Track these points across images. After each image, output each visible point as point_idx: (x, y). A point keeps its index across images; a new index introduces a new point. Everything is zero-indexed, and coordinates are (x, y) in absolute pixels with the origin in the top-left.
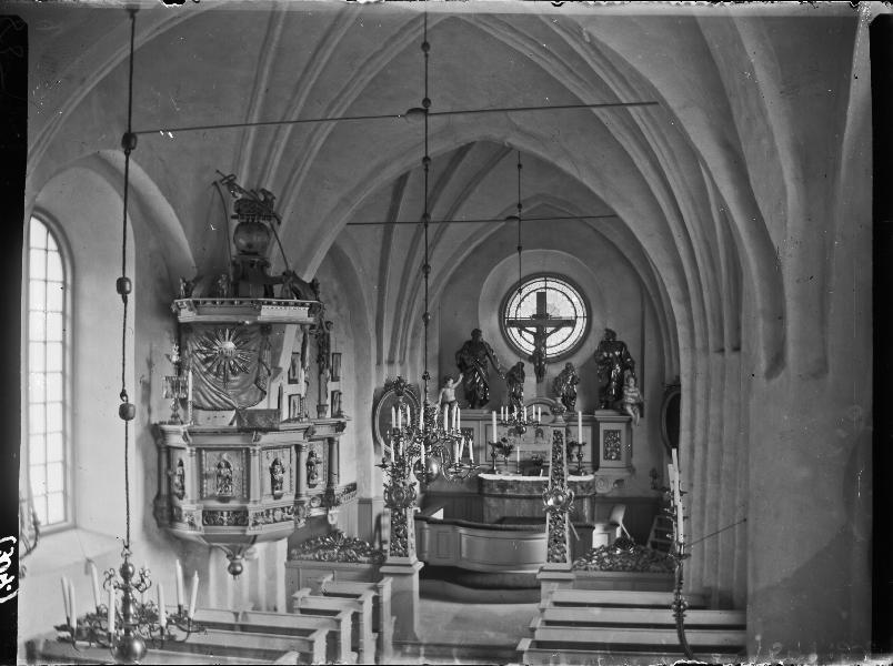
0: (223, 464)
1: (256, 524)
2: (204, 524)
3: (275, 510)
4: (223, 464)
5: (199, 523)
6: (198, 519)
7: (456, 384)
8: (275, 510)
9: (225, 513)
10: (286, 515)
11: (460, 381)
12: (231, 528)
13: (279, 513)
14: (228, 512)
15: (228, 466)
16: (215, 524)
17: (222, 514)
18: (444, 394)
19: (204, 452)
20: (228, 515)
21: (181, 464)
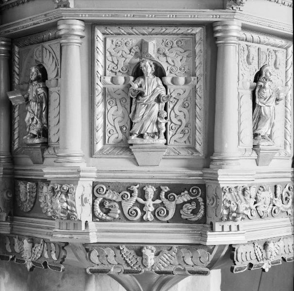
0: (149, 69)
1: (232, 216)
2: (94, 216)
3: (261, 188)
4: (149, 69)
5: (84, 213)
6: (84, 201)
9: (151, 191)
10: (278, 203)
12: (157, 226)
14: (159, 190)
15: (159, 73)
16: (124, 218)
17: (143, 194)
19: (99, 33)
20: (157, 196)
21: (43, 77)
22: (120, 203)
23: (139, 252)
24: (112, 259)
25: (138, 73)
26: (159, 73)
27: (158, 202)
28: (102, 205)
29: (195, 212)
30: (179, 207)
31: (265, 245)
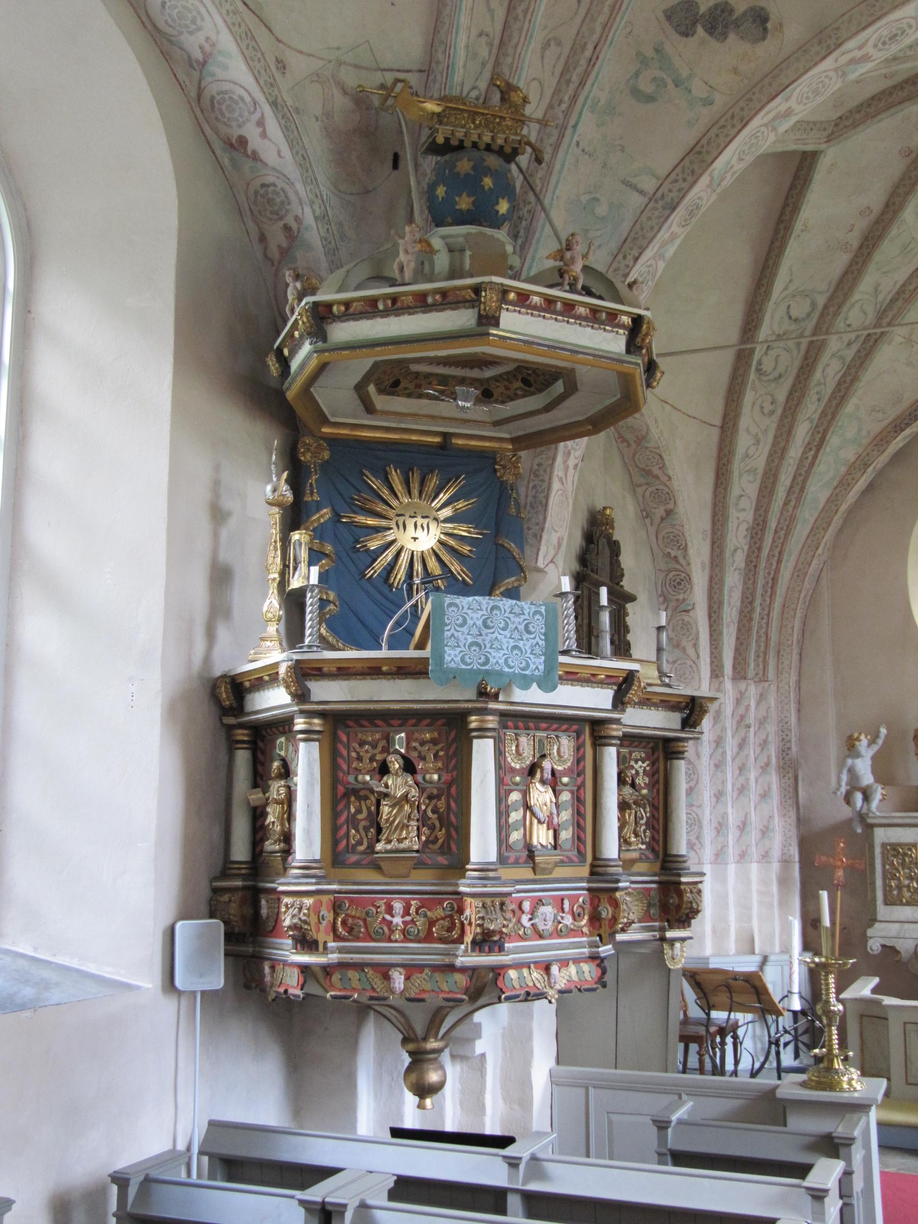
0: (396, 764)
4: (396, 764)
7: (875, 748)
8: (539, 902)
9: (398, 906)
10: (568, 920)
11: (880, 742)
13: (548, 911)
17: (390, 910)
18: (851, 771)
20: (406, 912)
22: (365, 921)
23: (387, 977)
24: (355, 984)
25: (384, 770)
26: (409, 767)
27: (408, 918)
28: (344, 923)
29: (450, 930)
30: (432, 923)
31: (547, 969)
